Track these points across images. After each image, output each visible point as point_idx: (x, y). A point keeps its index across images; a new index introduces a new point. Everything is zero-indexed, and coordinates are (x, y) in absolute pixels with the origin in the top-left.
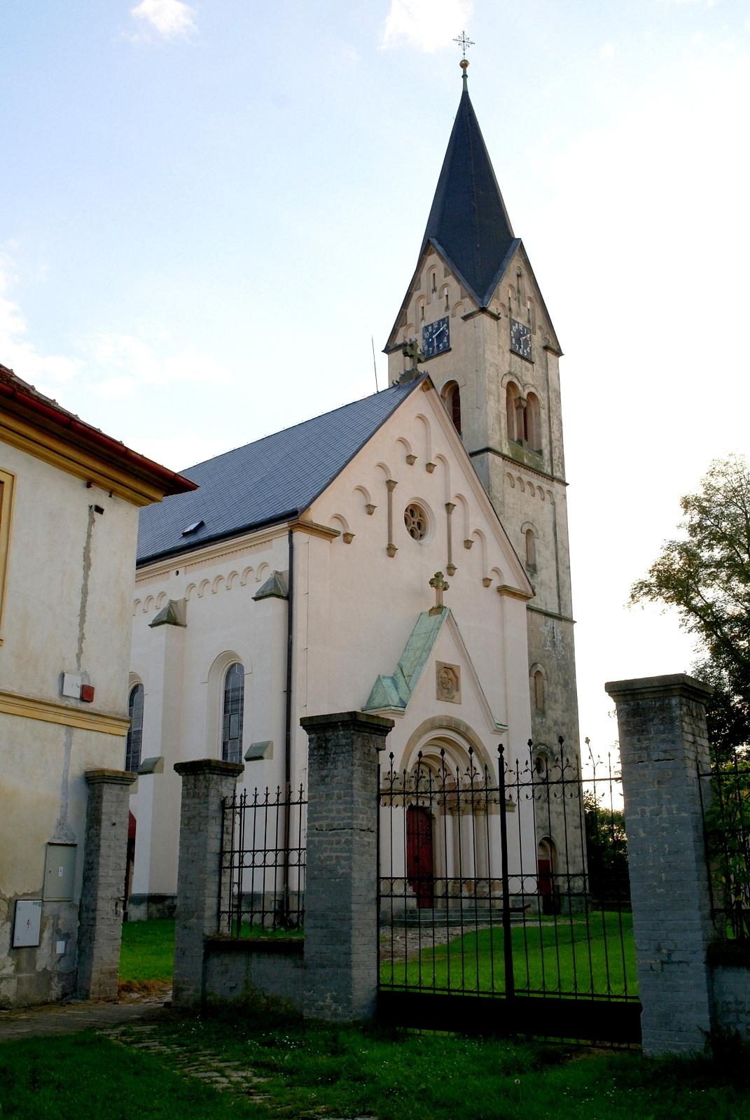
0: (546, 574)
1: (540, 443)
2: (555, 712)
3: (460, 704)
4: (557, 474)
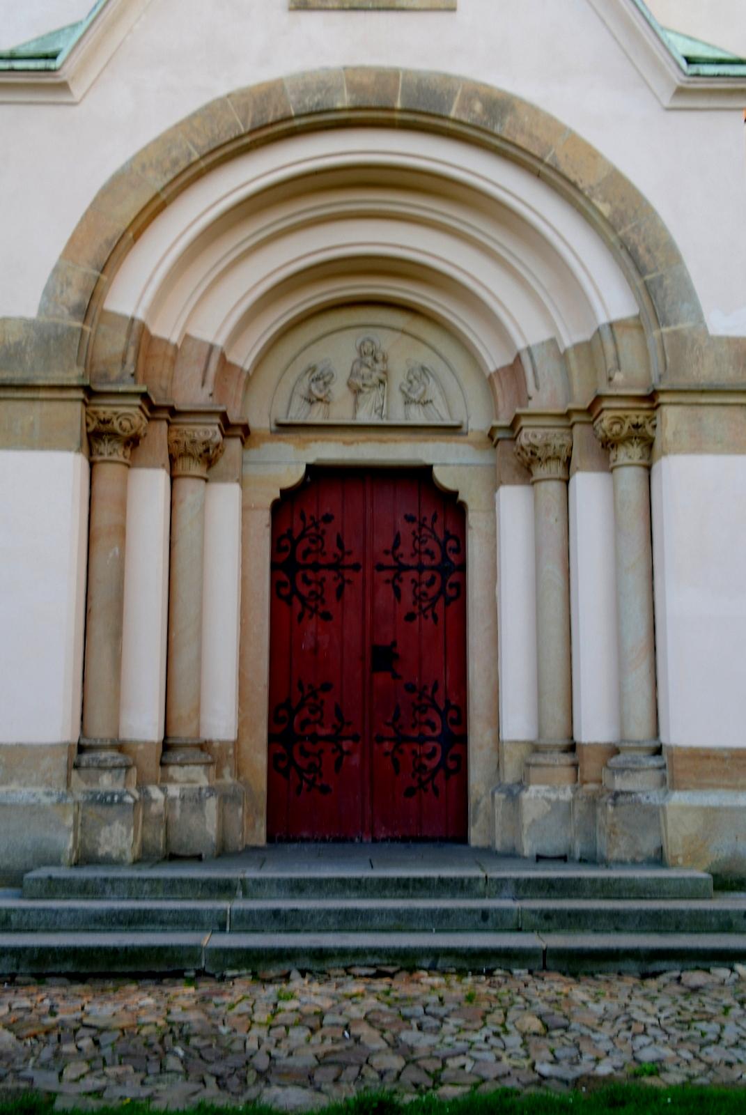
3: (452, 9)
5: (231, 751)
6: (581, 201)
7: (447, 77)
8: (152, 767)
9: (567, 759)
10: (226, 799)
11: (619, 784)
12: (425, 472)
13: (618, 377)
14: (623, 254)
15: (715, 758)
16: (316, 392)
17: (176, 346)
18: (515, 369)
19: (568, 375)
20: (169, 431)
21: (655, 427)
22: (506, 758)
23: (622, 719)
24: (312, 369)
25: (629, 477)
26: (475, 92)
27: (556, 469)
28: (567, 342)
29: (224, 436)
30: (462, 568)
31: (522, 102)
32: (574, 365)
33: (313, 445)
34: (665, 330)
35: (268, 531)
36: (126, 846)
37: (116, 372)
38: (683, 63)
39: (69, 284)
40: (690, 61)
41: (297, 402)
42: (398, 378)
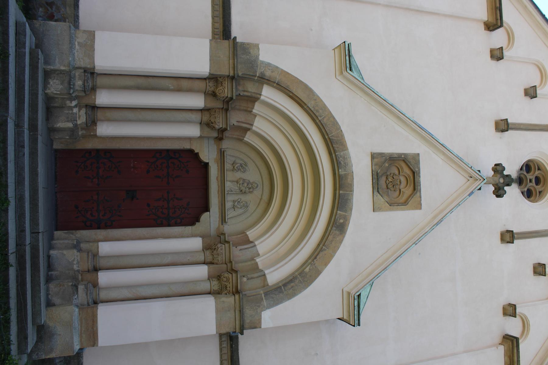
5: (92, 134)
6: (310, 261)
7: (351, 209)
8: (86, 101)
9: (91, 267)
10: (73, 131)
11: (81, 288)
12: (206, 208)
13: (245, 279)
14: (291, 278)
15: (93, 324)
16: (237, 166)
17: (252, 111)
18: (247, 241)
19: (246, 261)
20: (219, 108)
21: (226, 294)
22: (91, 244)
23: (109, 288)
24: (246, 165)
25: (207, 286)
26: (347, 220)
27: (209, 259)
28: (258, 260)
29: (218, 130)
30: (169, 225)
31: (344, 237)
32: (249, 263)
33: (216, 165)
34: (263, 295)
35: (182, 148)
36: (52, 90)
37: (240, 88)
38: (358, 294)
39: (272, 72)
40: (359, 296)
41: (233, 159)
42: (243, 198)
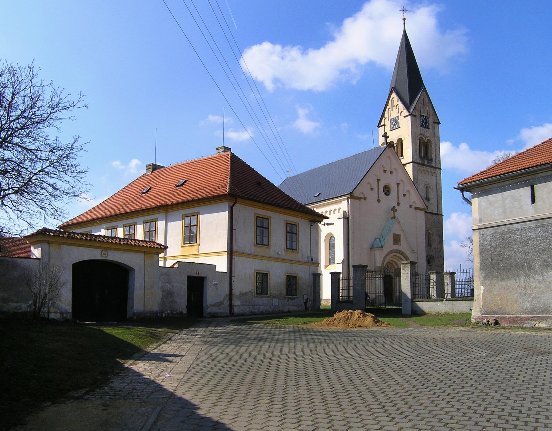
0: (433, 201)
1: (431, 156)
2: (435, 245)
4: (438, 166)
